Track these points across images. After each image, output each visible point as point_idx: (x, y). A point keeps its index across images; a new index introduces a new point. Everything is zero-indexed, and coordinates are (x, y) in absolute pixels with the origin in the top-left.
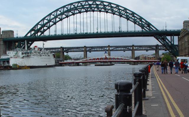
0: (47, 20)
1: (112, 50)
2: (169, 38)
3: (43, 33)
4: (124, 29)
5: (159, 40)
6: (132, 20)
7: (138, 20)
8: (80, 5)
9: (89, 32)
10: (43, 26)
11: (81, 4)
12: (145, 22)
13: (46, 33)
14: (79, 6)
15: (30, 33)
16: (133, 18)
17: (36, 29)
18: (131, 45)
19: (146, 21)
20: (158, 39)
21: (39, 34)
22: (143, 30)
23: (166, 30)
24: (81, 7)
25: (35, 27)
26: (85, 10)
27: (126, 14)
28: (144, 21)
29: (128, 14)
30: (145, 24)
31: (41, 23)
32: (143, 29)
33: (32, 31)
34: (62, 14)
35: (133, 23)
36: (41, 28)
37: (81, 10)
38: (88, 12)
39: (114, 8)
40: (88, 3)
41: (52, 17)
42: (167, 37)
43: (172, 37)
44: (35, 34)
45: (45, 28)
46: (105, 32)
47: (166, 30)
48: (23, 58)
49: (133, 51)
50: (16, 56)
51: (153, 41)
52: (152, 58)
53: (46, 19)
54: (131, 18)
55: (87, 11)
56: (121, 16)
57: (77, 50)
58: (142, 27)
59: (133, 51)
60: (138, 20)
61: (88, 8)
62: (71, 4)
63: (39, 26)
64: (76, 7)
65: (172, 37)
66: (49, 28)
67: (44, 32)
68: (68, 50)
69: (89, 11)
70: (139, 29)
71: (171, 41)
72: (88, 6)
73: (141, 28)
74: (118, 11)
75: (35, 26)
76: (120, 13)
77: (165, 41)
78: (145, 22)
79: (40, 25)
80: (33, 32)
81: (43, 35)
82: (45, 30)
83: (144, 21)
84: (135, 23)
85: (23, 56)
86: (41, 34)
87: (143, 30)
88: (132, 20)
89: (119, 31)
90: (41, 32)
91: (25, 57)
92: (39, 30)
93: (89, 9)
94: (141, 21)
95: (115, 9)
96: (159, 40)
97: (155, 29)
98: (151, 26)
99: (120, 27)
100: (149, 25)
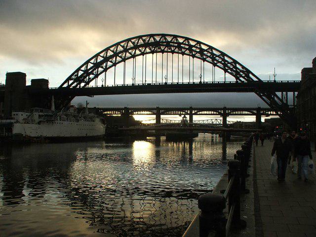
1: (196, 114)
2: (279, 94)
4: (208, 79)
5: (264, 97)
9: (149, 81)
14: (174, 46)
18: (222, 107)
19: (243, 67)
20: (261, 97)
21: (82, 84)
23: (275, 81)
43: (284, 93)
46: (178, 83)
47: (275, 81)
48: (40, 124)
49: (225, 116)
50: (26, 121)
51: (251, 98)
52: (252, 126)
58: (236, 74)
59: (225, 116)
65: (284, 93)
70: (231, 79)
71: (282, 98)
77: (274, 99)
85: (40, 121)
87: (237, 82)
89: (201, 82)
91: (44, 122)
96: (264, 97)
97: (255, 79)
98: (251, 75)
99: (202, 75)
100: (247, 72)
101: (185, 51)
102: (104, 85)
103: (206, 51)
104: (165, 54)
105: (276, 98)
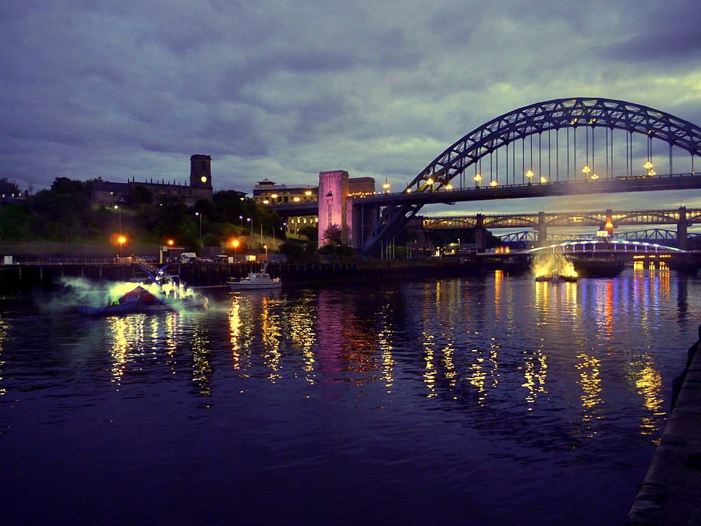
8: (540, 110)
10: (448, 166)
15: (416, 185)
24: (517, 125)
26: (554, 123)
34: (477, 145)
41: (454, 155)
55: (557, 127)
57: (519, 222)
62: (500, 119)
63: (438, 168)
66: (460, 170)
68: (498, 221)
72: (560, 114)
79: (439, 164)
82: (452, 176)
104: (545, 134)
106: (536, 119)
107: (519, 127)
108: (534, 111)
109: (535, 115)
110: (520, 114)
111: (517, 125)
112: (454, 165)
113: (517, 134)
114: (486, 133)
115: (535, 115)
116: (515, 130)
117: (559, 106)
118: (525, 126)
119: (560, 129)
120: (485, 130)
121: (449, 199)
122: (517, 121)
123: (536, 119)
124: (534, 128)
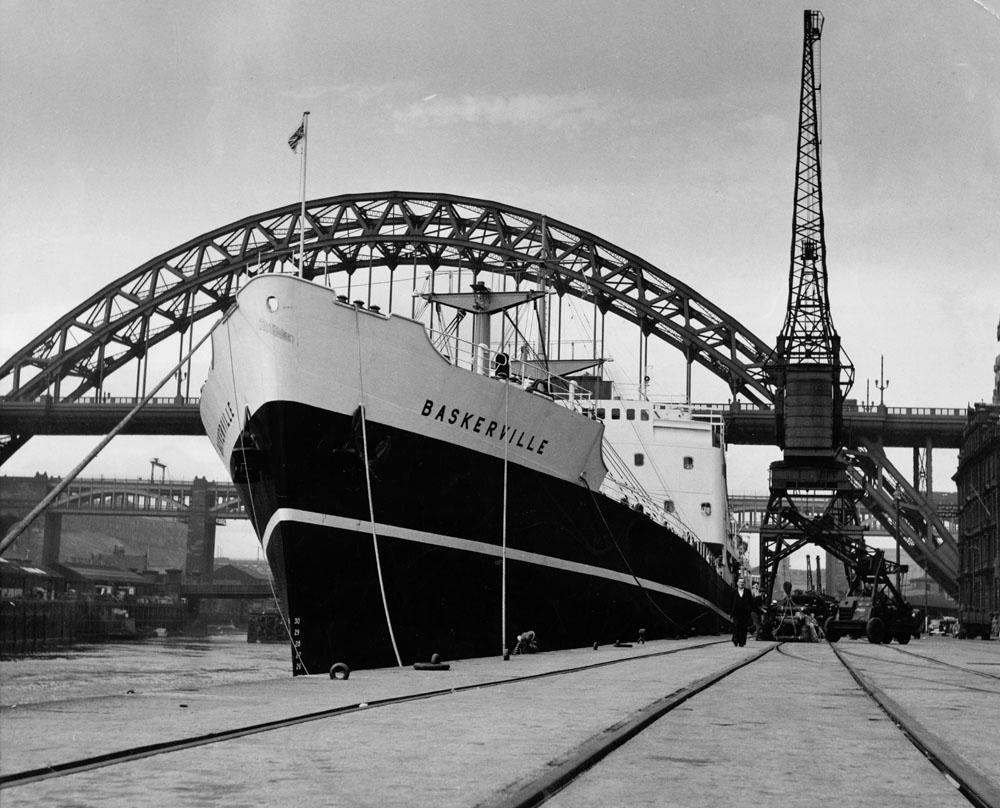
0: (132, 297)
3: (95, 379)
6: (672, 333)
7: (710, 337)
8: (351, 215)
11: (361, 212)
12: (754, 351)
13: (120, 386)
16: (680, 320)
17: (55, 351)
21: (70, 384)
22: (736, 405)
24: (337, 235)
25: (44, 339)
26: (385, 251)
27: (634, 294)
28: (750, 346)
29: (650, 296)
30: (757, 360)
31: (97, 317)
32: (740, 396)
33: (26, 363)
35: (681, 353)
36: (86, 350)
37: (357, 250)
38: (400, 267)
39: (521, 234)
40: (405, 208)
42: (887, 450)
44: (38, 385)
45: (114, 350)
47: (883, 408)
53: (124, 295)
54: (667, 320)
55: (392, 261)
56: (605, 305)
58: (736, 379)
60: (710, 337)
61: (400, 242)
63: (76, 337)
64: (324, 230)
66: (139, 350)
67: (107, 372)
69: (408, 260)
72: (401, 230)
73: (727, 385)
74: (589, 273)
75: (51, 332)
76: (597, 283)
78: (754, 351)
80: (29, 373)
81: (92, 392)
82: (111, 365)
83: (750, 346)
84: (692, 348)
86: (83, 389)
87: (736, 405)
88: (672, 333)
90: (83, 372)
92: (68, 363)
93: (409, 249)
94: (728, 341)
95: (525, 242)
101: (442, 250)
102: (184, 394)
103: (433, 219)
105: (884, 472)
106: (385, 230)
107: (342, 241)
108: (383, 208)
109: (385, 220)
110: (349, 210)
111: (337, 235)
112: (121, 333)
113: (334, 259)
114: (258, 238)
115: (385, 220)
116: (332, 246)
117: (397, 211)
118: (358, 243)
119: (399, 267)
120: (210, 249)
121: (101, 421)
122: (338, 227)
123: (385, 230)
124: (377, 254)
